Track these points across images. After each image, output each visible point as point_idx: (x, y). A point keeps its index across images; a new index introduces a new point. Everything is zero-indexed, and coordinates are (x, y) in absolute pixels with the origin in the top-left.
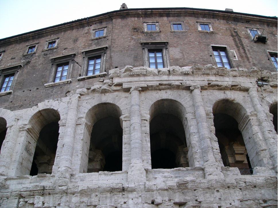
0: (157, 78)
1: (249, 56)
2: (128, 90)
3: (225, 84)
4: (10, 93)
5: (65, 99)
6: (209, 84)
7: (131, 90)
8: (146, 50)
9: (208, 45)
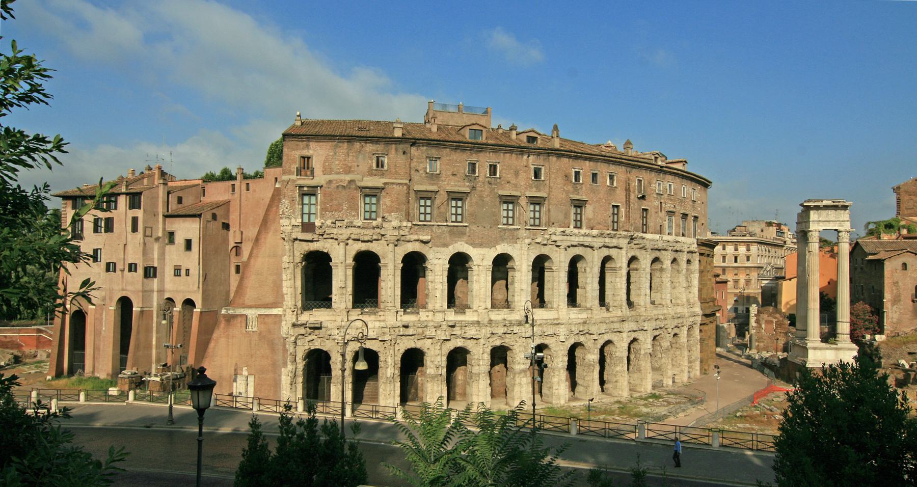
1: (631, 214)
5: (518, 246)
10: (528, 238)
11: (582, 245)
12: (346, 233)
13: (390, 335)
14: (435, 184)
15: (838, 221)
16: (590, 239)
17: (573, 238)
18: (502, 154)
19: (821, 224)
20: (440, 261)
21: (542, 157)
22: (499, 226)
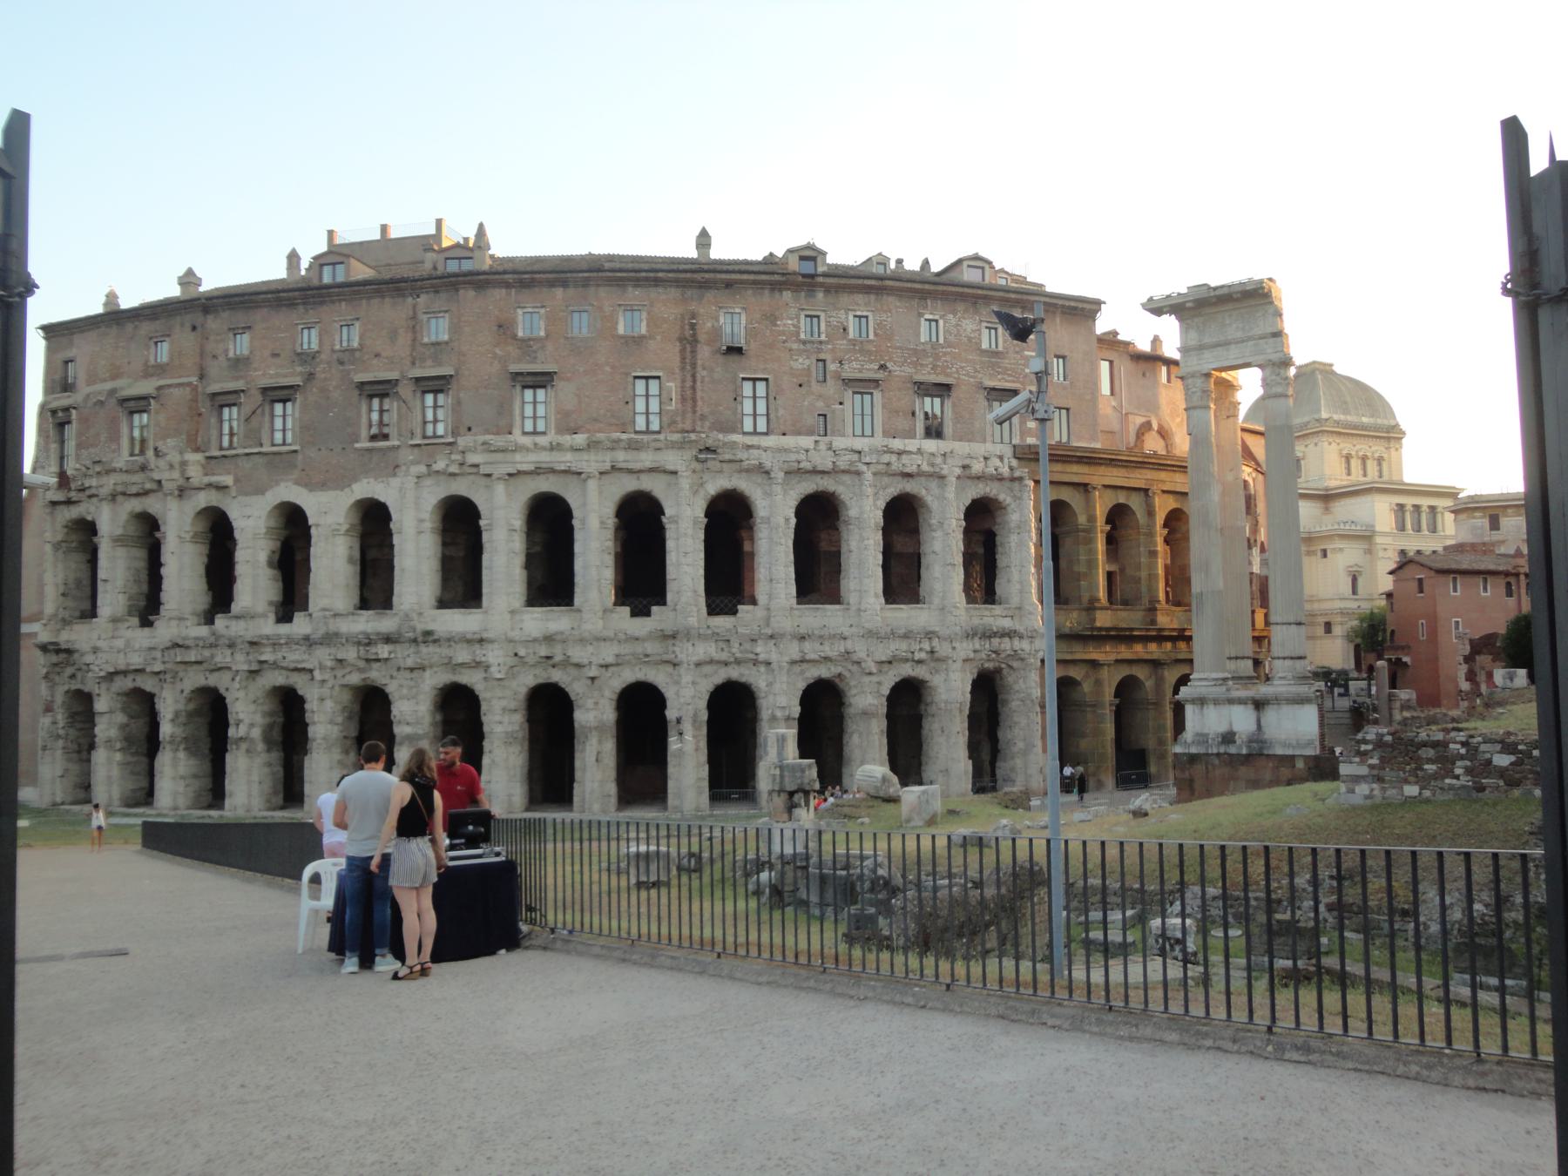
0: (533, 457)
1: (699, 394)
2: (489, 475)
3: (638, 466)
4: (295, 451)
6: (613, 467)
7: (494, 477)
8: (518, 388)
9: (627, 374)
10: (418, 463)
11: (553, 471)
12: (109, 483)
13: (164, 663)
14: (241, 377)
15: (1250, 339)
16: (569, 456)
17: (518, 457)
18: (364, 301)
19: (1207, 354)
20: (251, 522)
21: (443, 296)
22: (357, 445)
